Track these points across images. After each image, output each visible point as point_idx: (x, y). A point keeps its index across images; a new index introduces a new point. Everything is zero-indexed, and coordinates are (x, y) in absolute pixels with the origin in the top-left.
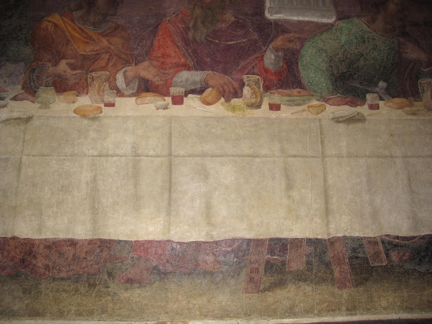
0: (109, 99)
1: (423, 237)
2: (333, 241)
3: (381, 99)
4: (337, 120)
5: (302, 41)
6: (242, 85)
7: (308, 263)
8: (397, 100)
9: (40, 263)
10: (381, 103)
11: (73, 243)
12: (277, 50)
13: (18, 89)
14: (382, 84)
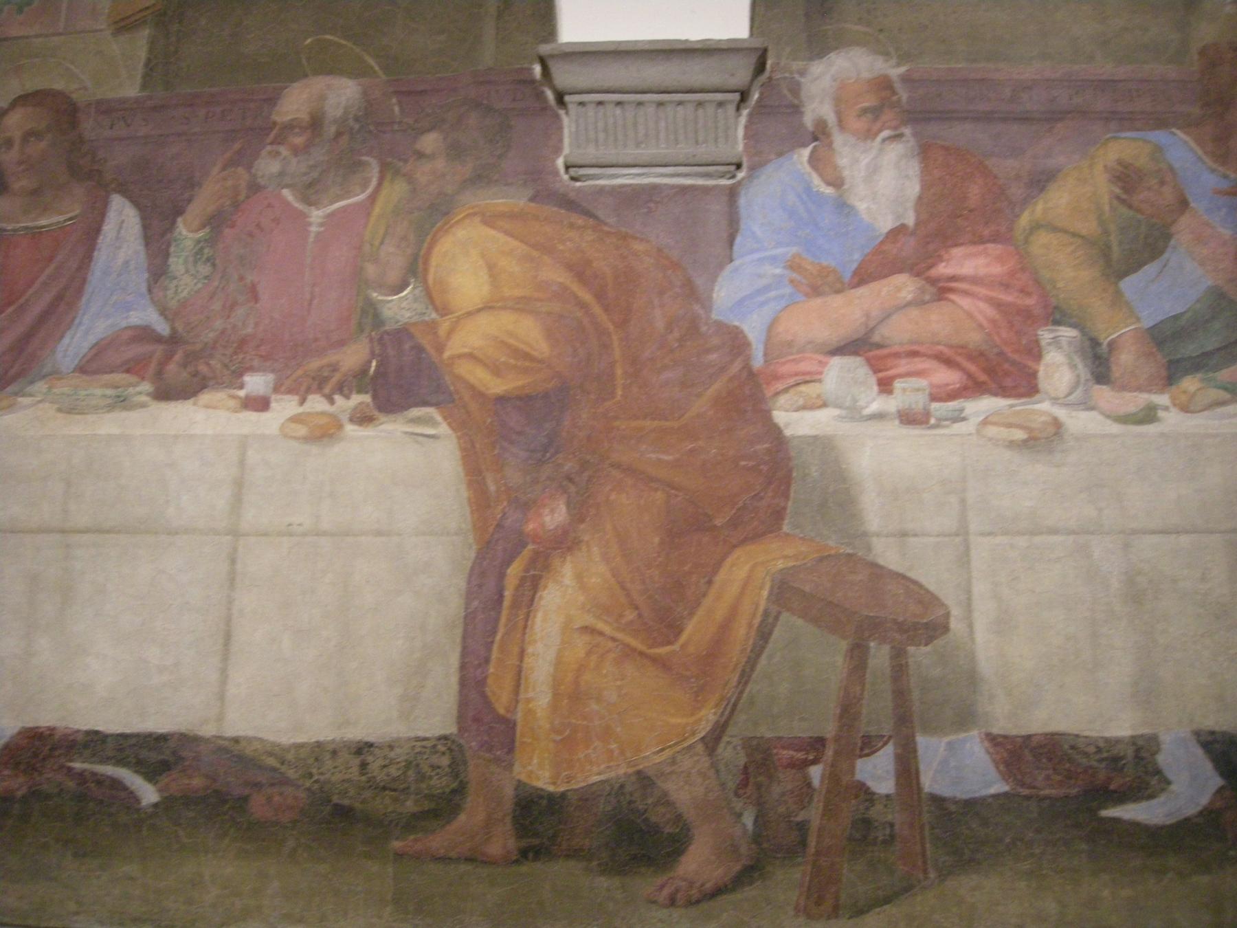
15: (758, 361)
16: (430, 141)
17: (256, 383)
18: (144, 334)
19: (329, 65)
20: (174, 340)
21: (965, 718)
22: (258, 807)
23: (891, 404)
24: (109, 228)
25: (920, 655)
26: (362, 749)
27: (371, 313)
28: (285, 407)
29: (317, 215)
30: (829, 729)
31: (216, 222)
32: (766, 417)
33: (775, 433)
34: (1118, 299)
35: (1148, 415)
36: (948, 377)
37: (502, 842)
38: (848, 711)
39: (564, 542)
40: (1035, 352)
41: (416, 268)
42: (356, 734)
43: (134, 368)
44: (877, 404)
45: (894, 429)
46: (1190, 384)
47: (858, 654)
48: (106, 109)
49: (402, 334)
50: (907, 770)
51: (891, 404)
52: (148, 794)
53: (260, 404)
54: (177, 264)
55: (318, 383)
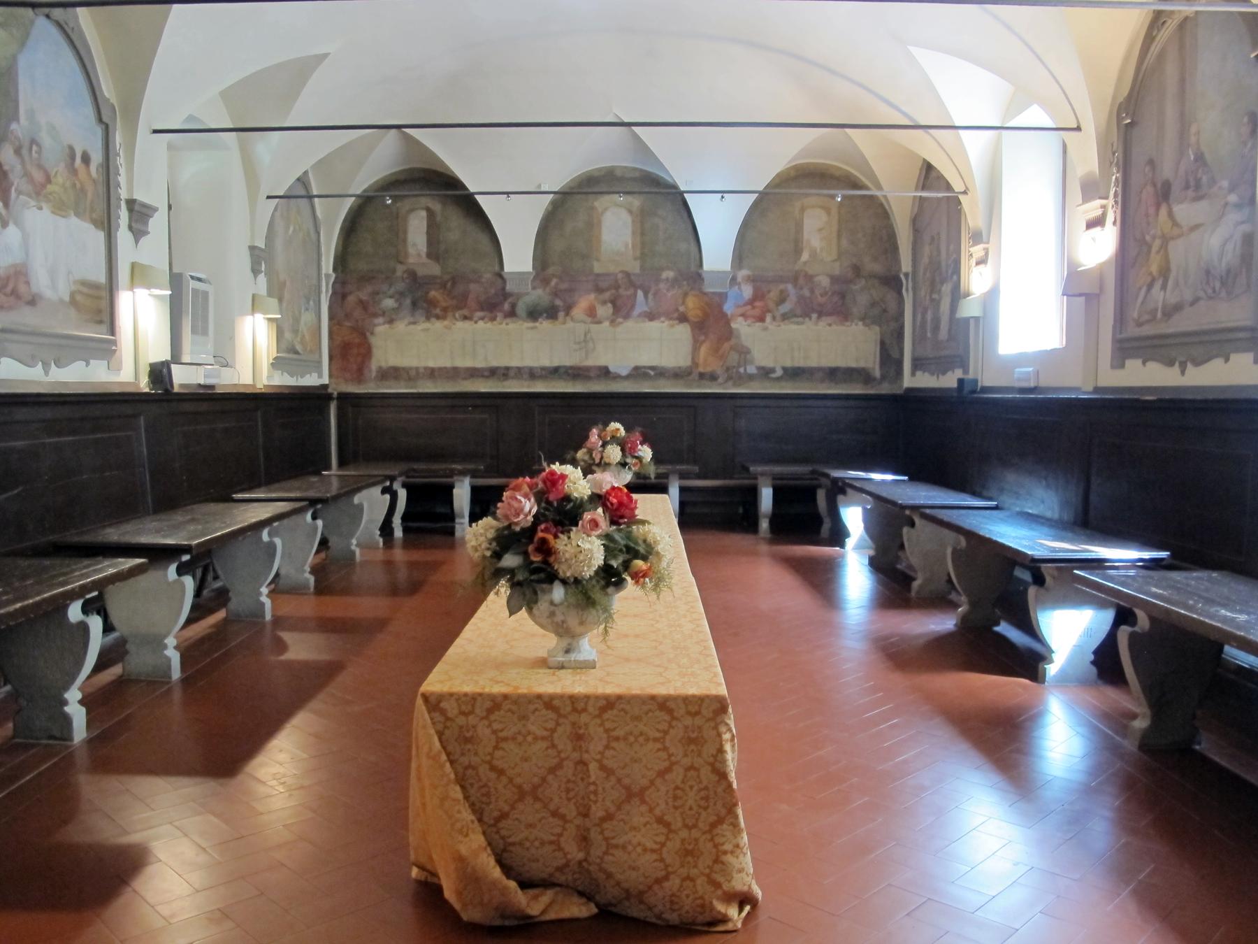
0: (455, 322)
1: (553, 367)
2: (524, 368)
3: (544, 320)
4: (528, 328)
5: (518, 299)
6: (496, 316)
7: (516, 374)
8: (550, 321)
9: (436, 374)
10: (544, 322)
11: (445, 368)
12: (510, 303)
13: (423, 319)
14: (545, 315)
15: (729, 316)
16: (685, 283)
17: (662, 319)
18: (645, 312)
19: (668, 268)
20: (650, 313)
21: (752, 362)
22: (667, 375)
23: (746, 323)
24: (638, 294)
25: (748, 356)
26: (680, 368)
27: (677, 310)
28: (667, 323)
29: (669, 294)
30: (736, 365)
31: (655, 294)
32: (730, 325)
33: (731, 327)
34: (778, 309)
35: (779, 326)
36: (753, 320)
37: (697, 378)
38: (739, 363)
39: (704, 341)
40: (765, 317)
41: (683, 303)
42: (679, 365)
43: (645, 316)
44: (744, 323)
45: (746, 327)
46: (786, 321)
47: (740, 356)
48: (634, 274)
49: (682, 313)
50: (745, 370)
51: (746, 323)
52: (652, 373)
53: (663, 322)
54: (650, 300)
55: (671, 319)
